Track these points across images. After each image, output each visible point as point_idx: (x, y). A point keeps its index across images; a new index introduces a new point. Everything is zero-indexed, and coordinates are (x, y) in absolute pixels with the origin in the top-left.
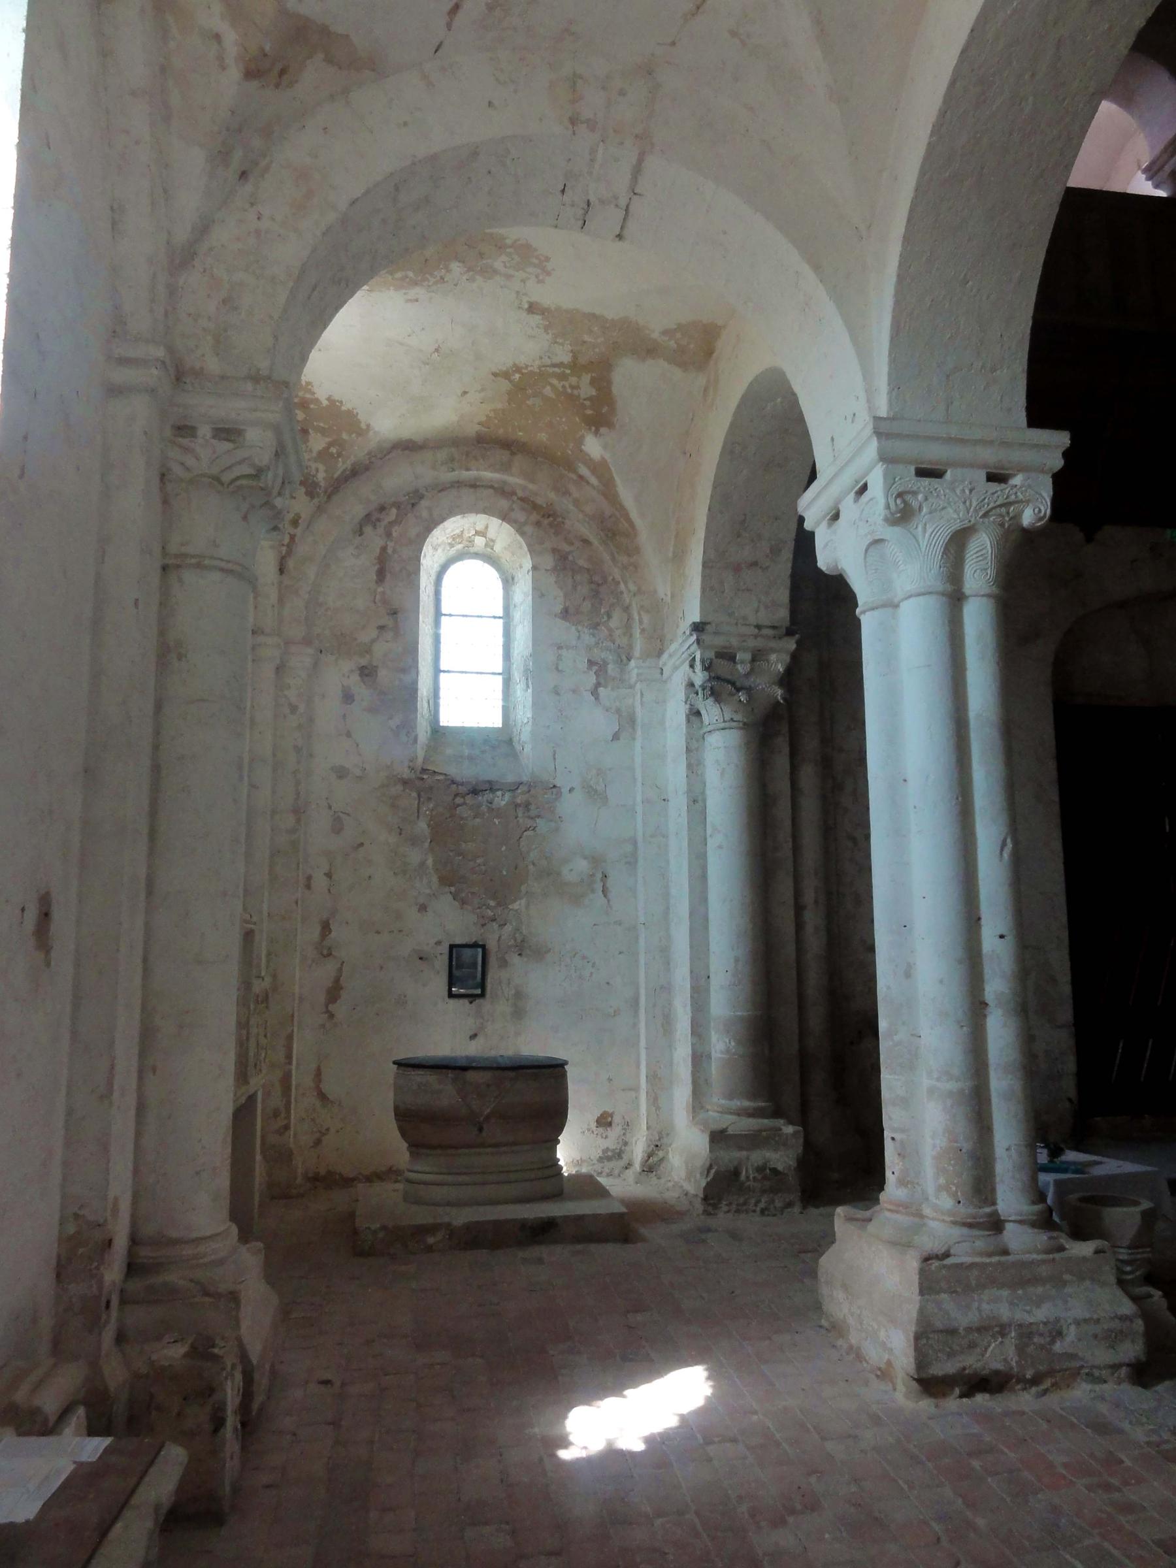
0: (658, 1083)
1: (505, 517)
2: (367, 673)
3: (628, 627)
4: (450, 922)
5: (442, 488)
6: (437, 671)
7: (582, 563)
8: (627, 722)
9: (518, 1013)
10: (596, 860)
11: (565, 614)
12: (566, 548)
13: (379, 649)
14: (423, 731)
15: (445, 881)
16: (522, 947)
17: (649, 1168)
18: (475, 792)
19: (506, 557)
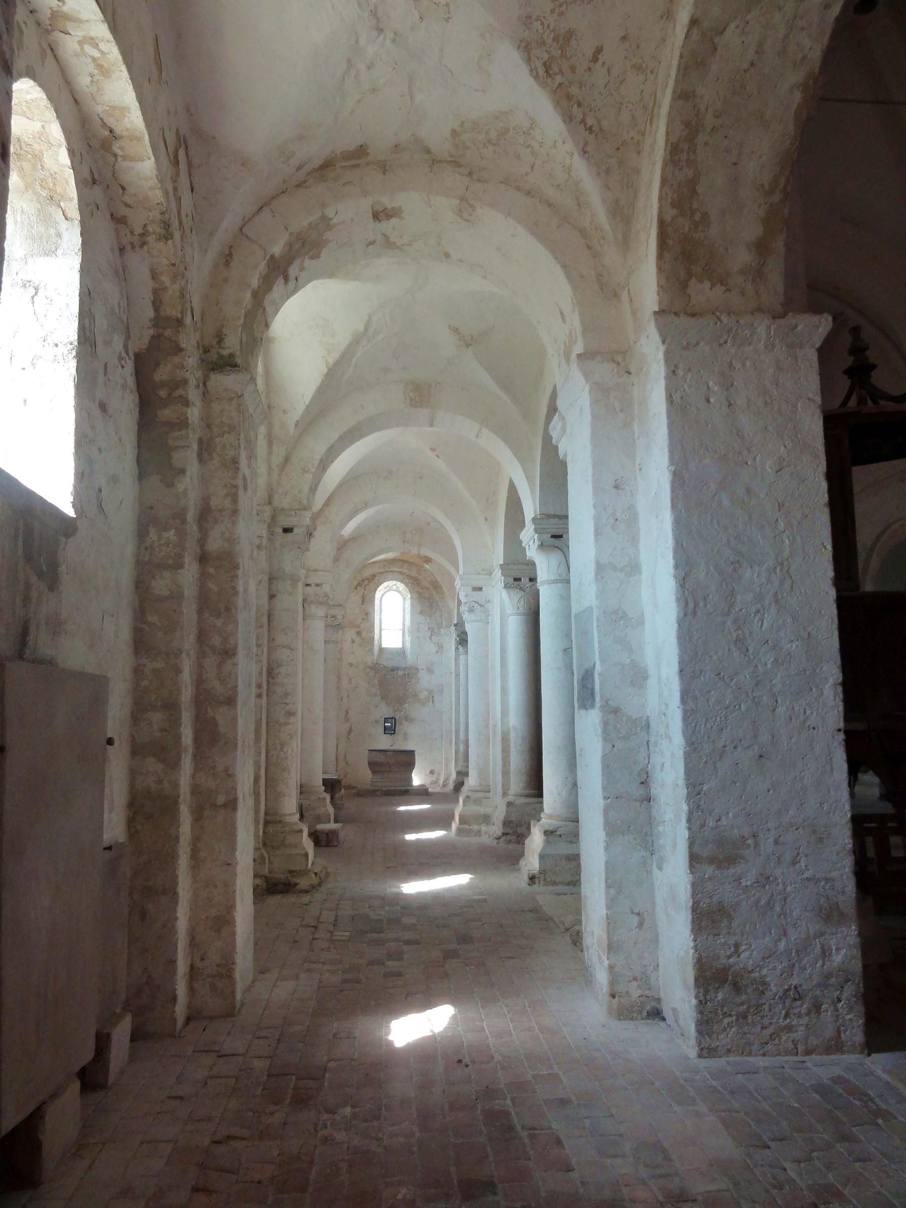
0: (447, 760)
1: (401, 582)
2: (359, 633)
3: (441, 616)
4: (385, 711)
5: (383, 573)
6: (381, 630)
7: (426, 595)
8: (440, 648)
9: (406, 737)
10: (430, 691)
11: (421, 613)
12: (421, 590)
13: (362, 626)
14: (376, 649)
15: (382, 698)
16: (407, 718)
17: (444, 786)
18: (392, 670)
19: (403, 592)
